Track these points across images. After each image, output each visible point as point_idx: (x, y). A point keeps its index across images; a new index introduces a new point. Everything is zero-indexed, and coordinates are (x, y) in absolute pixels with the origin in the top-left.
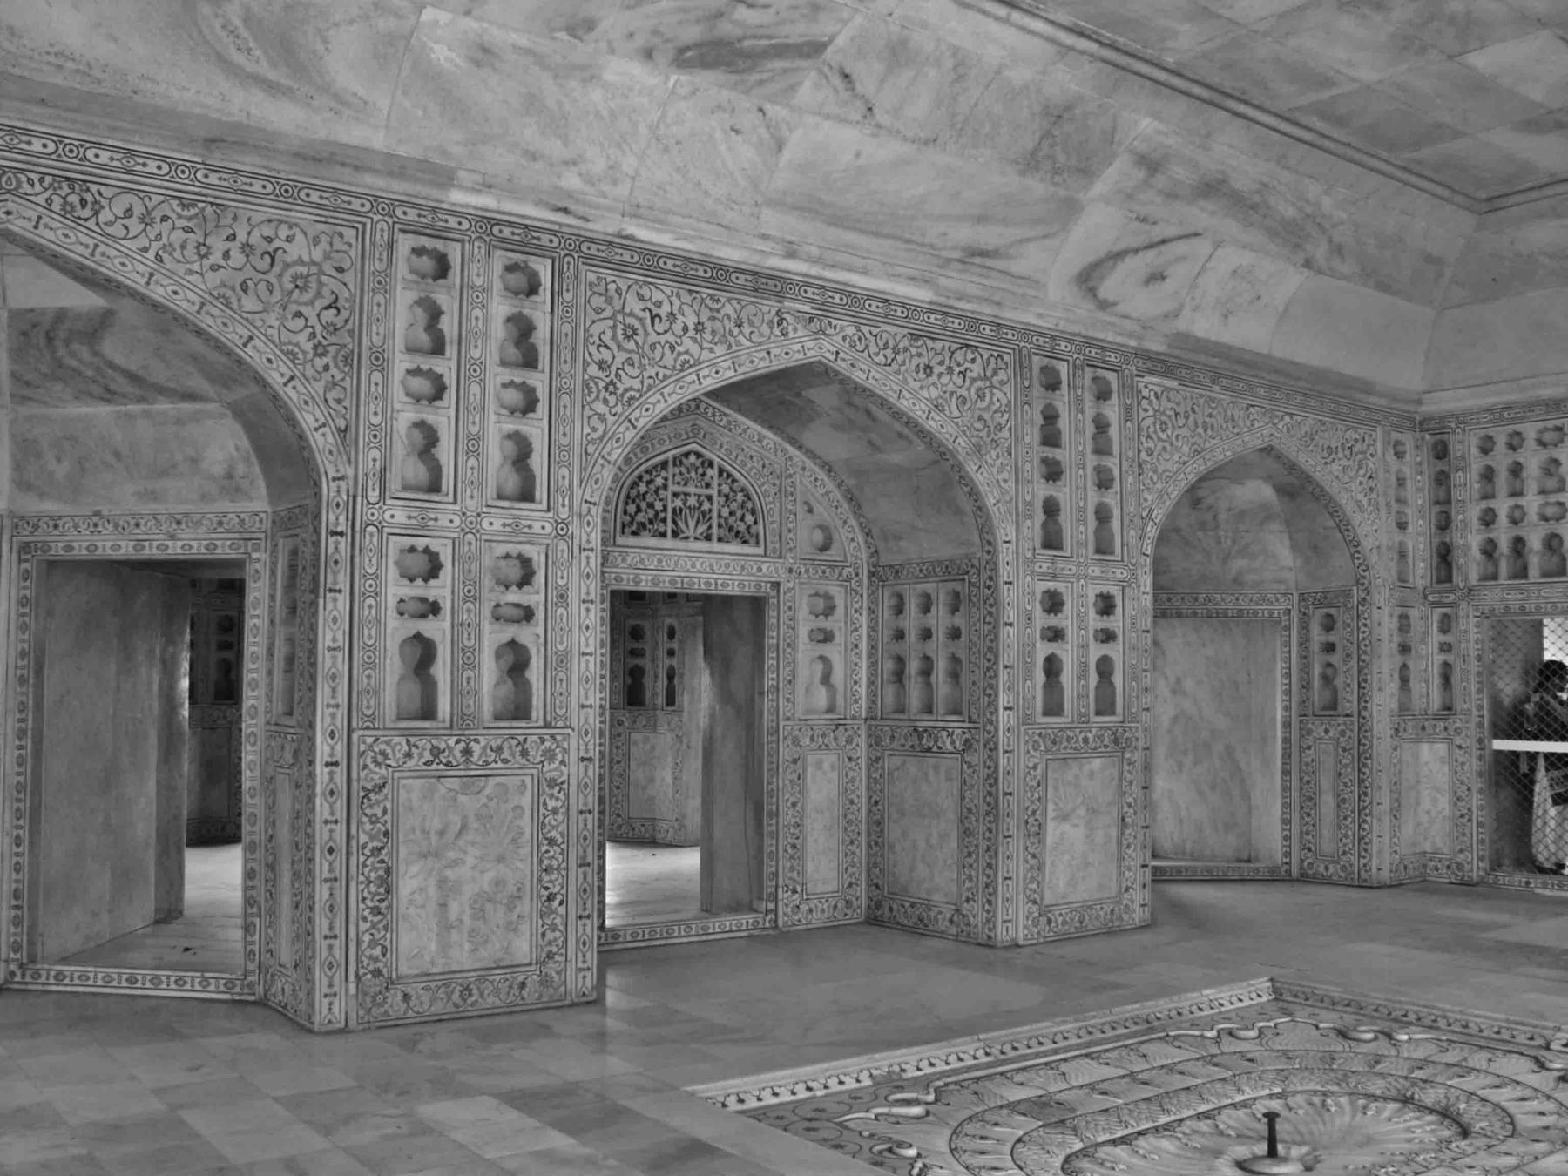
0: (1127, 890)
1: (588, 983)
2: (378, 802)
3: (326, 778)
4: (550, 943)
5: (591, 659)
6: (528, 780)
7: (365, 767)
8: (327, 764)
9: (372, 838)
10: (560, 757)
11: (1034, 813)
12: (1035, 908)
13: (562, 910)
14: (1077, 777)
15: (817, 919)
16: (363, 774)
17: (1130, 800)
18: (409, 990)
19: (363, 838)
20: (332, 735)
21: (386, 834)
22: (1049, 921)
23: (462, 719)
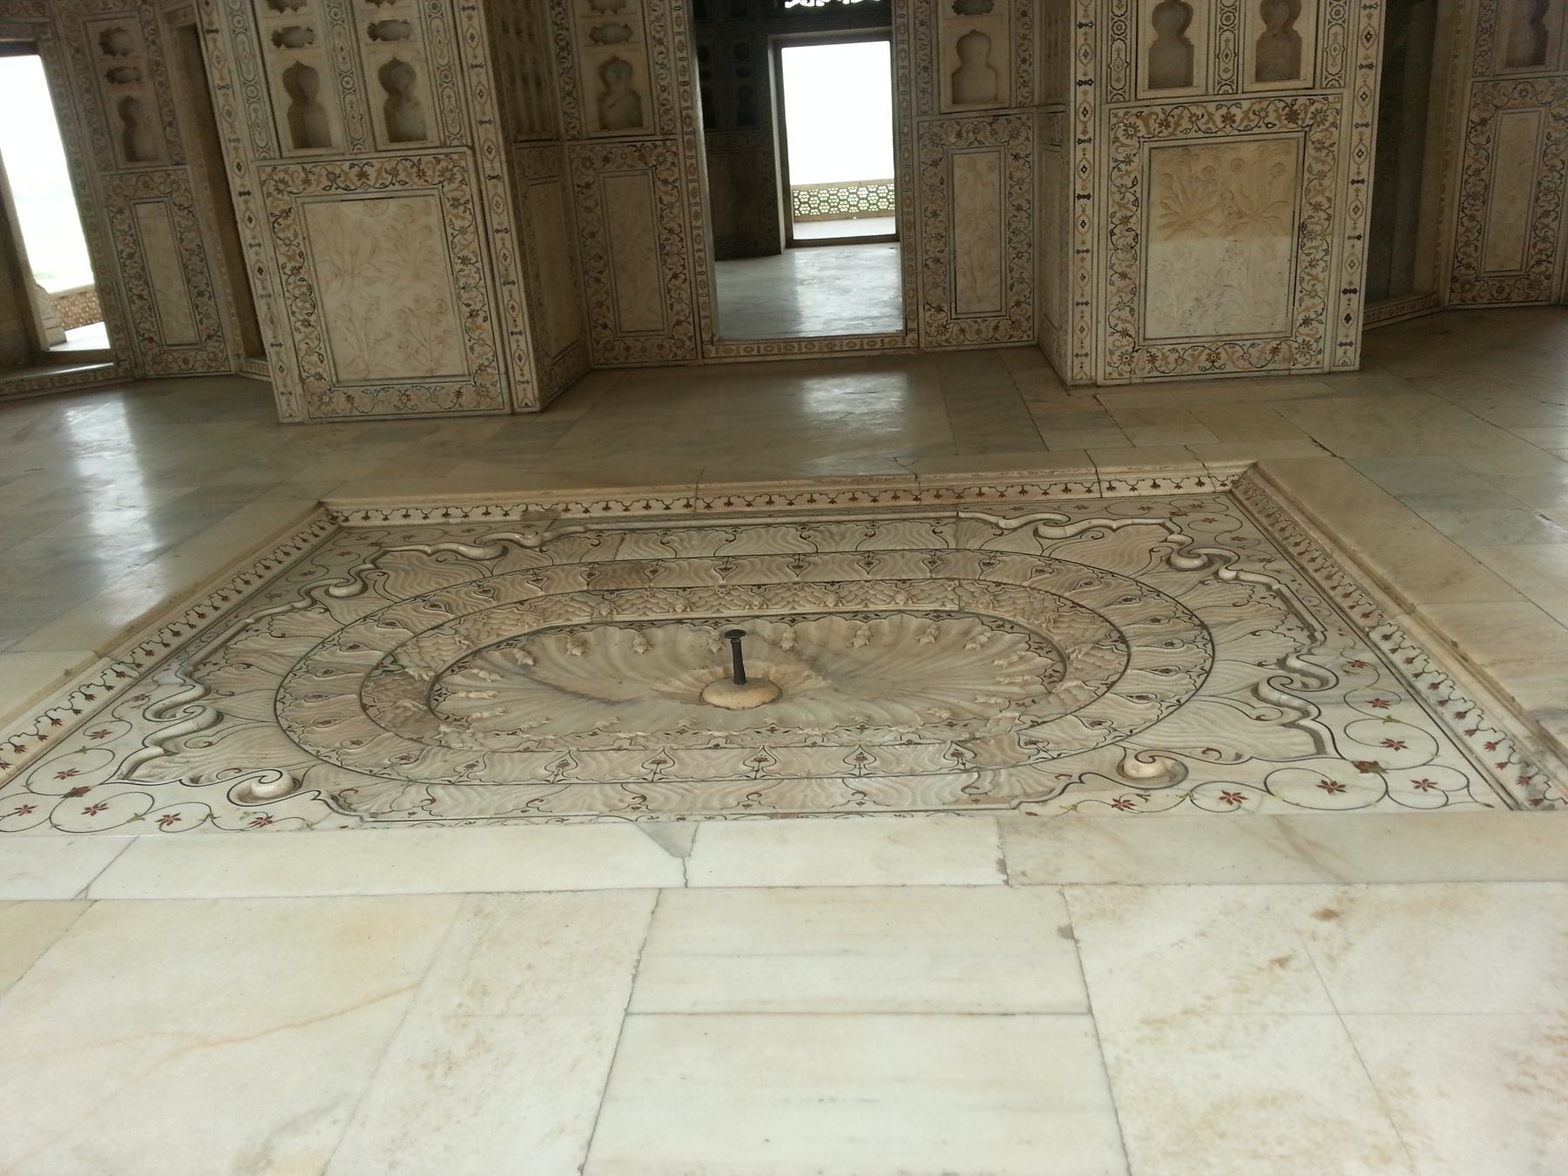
0: (1306, 322)
1: (530, 396)
2: (289, 226)
3: (243, 207)
4: (480, 356)
5: (483, 71)
6: (433, 201)
7: (269, 194)
8: (241, 194)
9: (291, 258)
10: (459, 177)
11: (1125, 220)
12: (1125, 341)
13: (487, 325)
14: (1206, 170)
15: (971, 340)
16: (268, 202)
17: (1320, 198)
18: (350, 392)
19: (282, 260)
20: (239, 167)
21: (301, 254)
22: (1153, 358)
23: (353, 143)
